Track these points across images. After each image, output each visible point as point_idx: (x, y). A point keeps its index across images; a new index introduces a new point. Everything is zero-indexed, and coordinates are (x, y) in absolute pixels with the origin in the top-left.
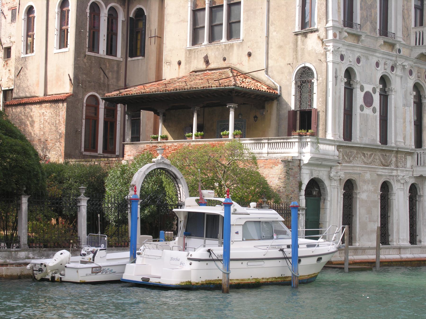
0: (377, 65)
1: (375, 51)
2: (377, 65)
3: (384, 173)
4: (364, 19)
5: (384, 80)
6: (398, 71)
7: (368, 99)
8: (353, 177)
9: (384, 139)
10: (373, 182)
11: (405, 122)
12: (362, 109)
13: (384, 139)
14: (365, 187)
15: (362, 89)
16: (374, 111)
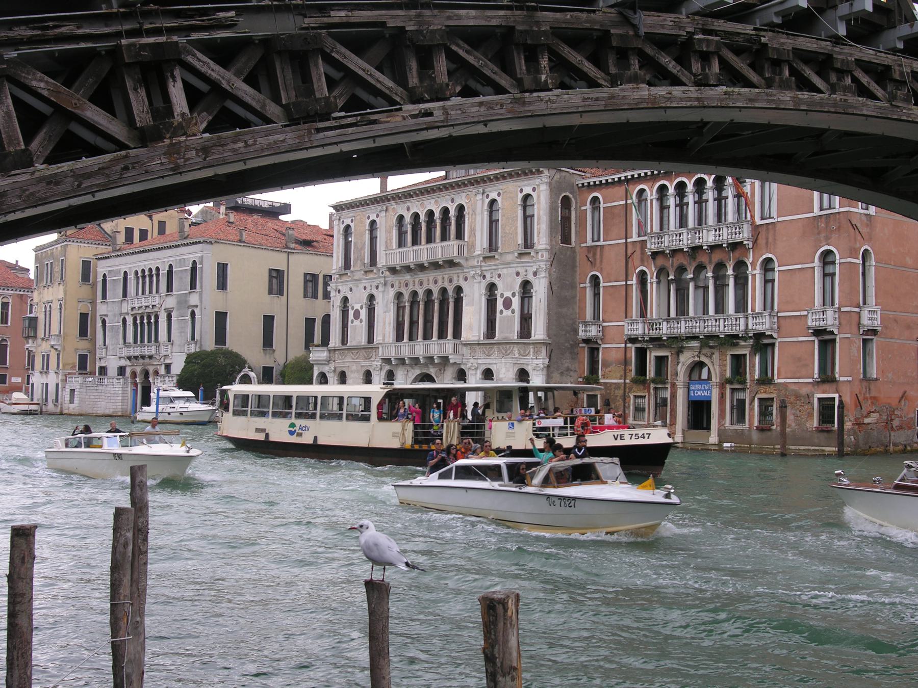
0: (365, 288)
1: (360, 280)
2: (365, 288)
3: (366, 364)
4: (356, 260)
5: (371, 298)
6: (380, 288)
7: (357, 315)
8: (344, 369)
9: (370, 339)
10: (358, 371)
11: (384, 324)
12: (352, 322)
13: (370, 339)
14: (352, 375)
15: (353, 308)
16: (361, 321)
